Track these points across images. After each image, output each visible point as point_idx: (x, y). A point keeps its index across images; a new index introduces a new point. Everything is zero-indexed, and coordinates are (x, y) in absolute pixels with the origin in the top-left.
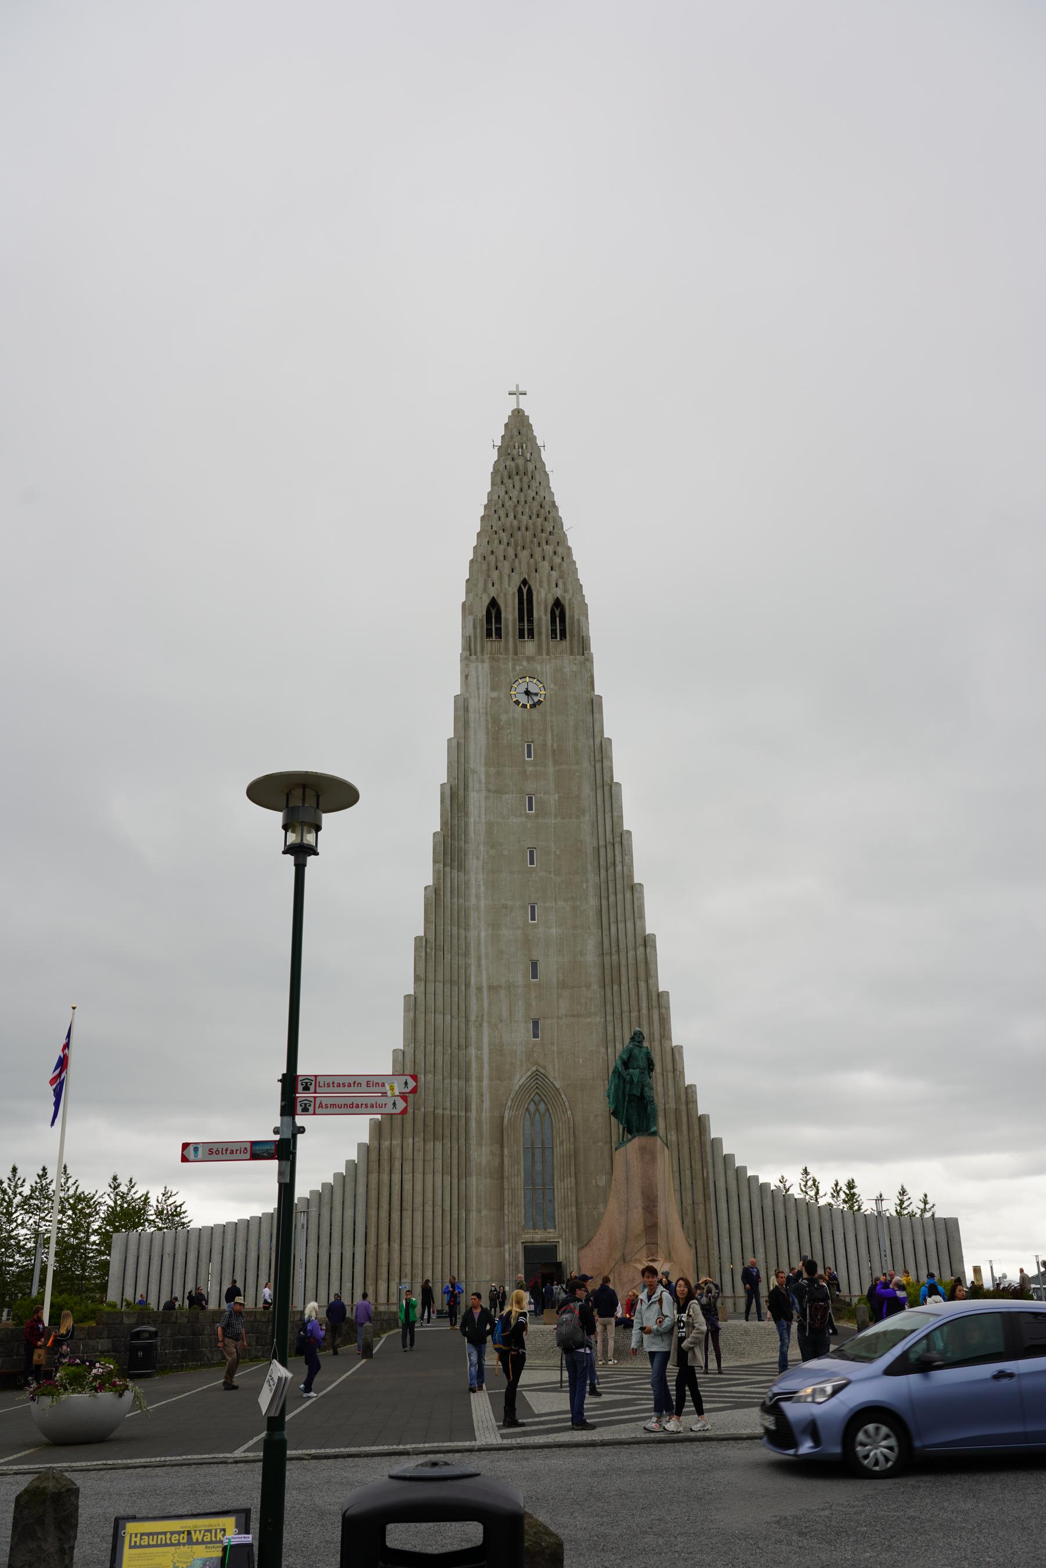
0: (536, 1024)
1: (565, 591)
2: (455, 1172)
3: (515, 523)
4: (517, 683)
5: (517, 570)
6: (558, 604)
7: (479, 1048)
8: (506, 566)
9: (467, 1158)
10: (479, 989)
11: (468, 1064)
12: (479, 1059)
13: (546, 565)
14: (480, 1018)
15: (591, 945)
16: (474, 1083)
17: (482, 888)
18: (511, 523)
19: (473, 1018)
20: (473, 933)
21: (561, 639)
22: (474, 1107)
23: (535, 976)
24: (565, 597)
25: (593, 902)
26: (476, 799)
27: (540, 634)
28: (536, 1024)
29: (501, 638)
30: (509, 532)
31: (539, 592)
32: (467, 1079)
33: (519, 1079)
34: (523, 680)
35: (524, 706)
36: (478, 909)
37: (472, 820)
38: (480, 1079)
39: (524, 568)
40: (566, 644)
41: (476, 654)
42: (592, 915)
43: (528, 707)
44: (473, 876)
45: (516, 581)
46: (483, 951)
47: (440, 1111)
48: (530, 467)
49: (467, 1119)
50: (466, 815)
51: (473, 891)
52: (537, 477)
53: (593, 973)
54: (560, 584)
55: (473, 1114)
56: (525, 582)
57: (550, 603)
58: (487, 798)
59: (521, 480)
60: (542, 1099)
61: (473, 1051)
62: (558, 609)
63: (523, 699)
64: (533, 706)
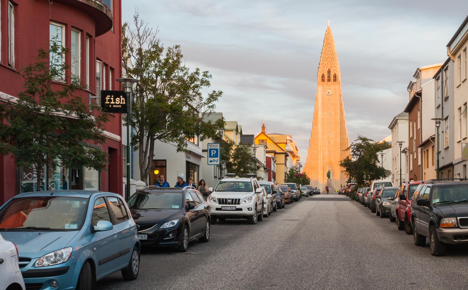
0: (329, 152)
1: (337, 72)
3: (328, 56)
5: (328, 67)
7: (320, 155)
8: (326, 66)
9: (318, 172)
10: (320, 146)
11: (318, 158)
12: (320, 157)
13: (333, 66)
14: (320, 151)
15: (339, 138)
16: (319, 161)
17: (321, 129)
19: (319, 150)
20: (319, 136)
22: (319, 165)
26: (320, 113)
32: (318, 160)
33: (327, 160)
36: (320, 132)
37: (319, 117)
38: (320, 160)
39: (329, 67)
40: (336, 82)
42: (339, 134)
44: (319, 127)
46: (321, 139)
47: (314, 166)
48: (331, 42)
49: (318, 167)
50: (318, 116)
51: (319, 129)
52: (332, 45)
53: (339, 143)
54: (336, 70)
55: (319, 166)
56: (329, 69)
57: (334, 74)
58: (322, 112)
61: (319, 156)
62: (335, 76)
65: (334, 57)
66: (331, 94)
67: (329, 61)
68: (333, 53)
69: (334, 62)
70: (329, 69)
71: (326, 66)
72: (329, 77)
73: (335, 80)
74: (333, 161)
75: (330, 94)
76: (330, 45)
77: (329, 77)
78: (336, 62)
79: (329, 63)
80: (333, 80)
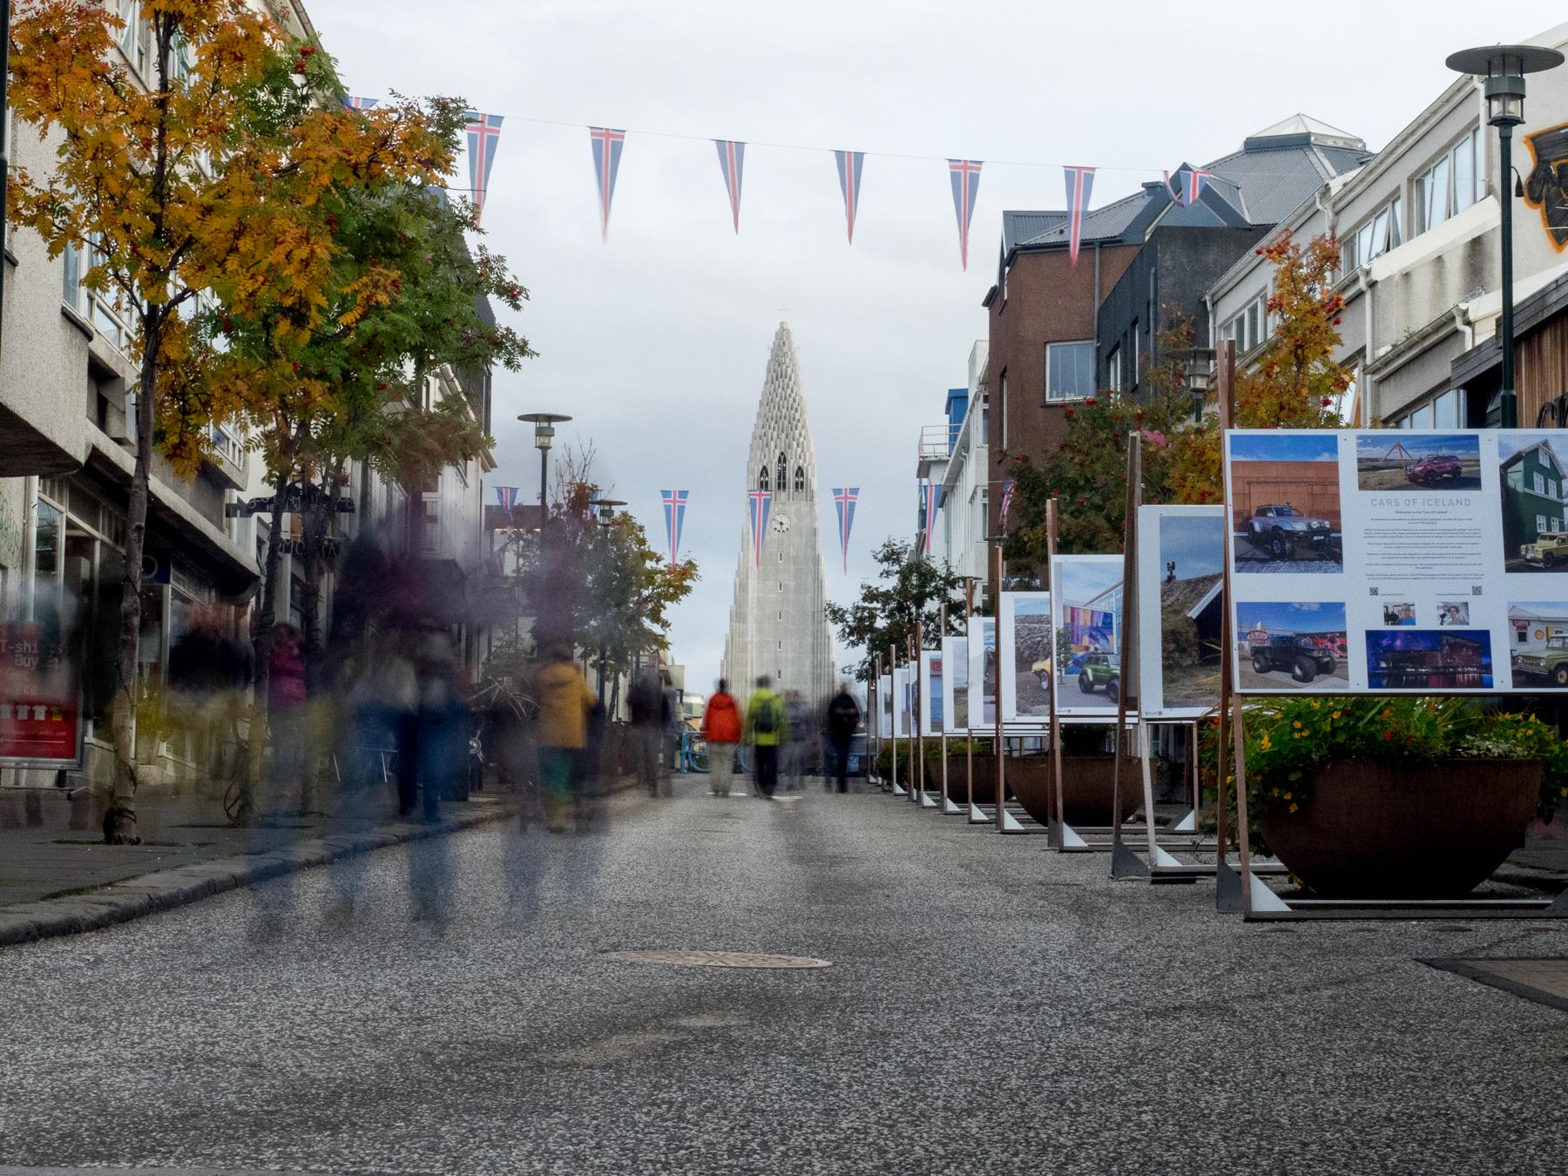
6: (800, 468)
8: (773, 444)
13: (795, 444)
15: (808, 662)
25: (810, 640)
26: (752, 583)
42: (809, 646)
48: (789, 371)
63: (778, 527)
65: (798, 417)
68: (795, 405)
69: (797, 432)
72: (782, 475)
73: (799, 486)
75: (784, 528)
77: (782, 475)
78: (803, 432)
79: (783, 436)
80: (792, 485)
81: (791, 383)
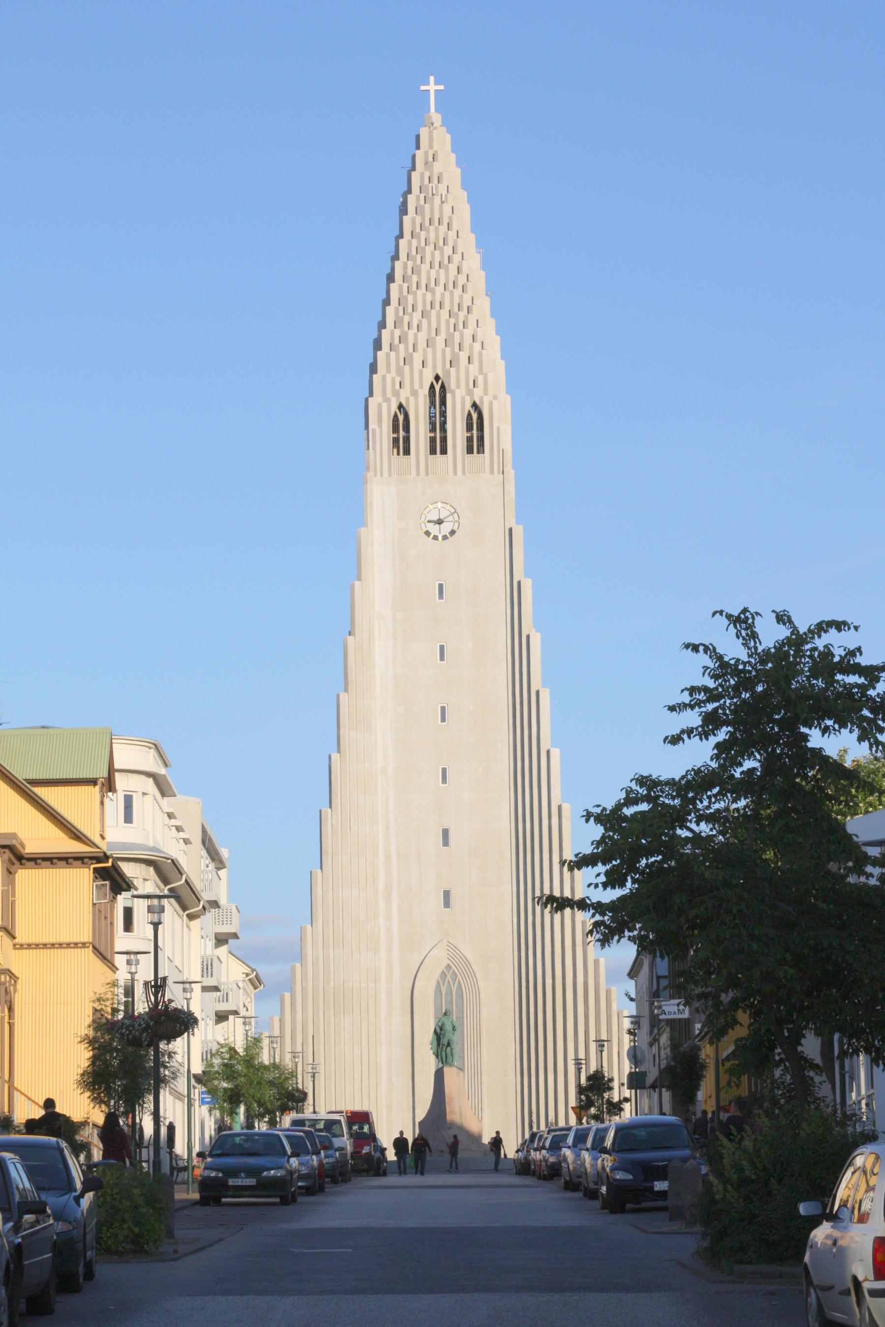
0: (447, 894)
2: (365, 1042)
3: (429, 296)
4: (428, 510)
5: (429, 363)
13: (463, 356)
18: (424, 296)
21: (478, 452)
23: (446, 842)
24: (481, 399)
27: (454, 447)
28: (447, 894)
29: (409, 454)
30: (420, 308)
31: (453, 393)
34: (435, 505)
35: (435, 538)
41: (382, 475)
43: (440, 538)
45: (429, 379)
56: (437, 378)
59: (437, 230)
60: (454, 972)
63: (434, 529)
64: (445, 538)
65: (467, 302)
66: (453, 532)
67: (434, 326)
68: (462, 280)
69: (468, 333)
70: (437, 378)
71: (417, 358)
74: (470, 956)
75: (446, 528)
76: (443, 229)
81: (452, 235)
